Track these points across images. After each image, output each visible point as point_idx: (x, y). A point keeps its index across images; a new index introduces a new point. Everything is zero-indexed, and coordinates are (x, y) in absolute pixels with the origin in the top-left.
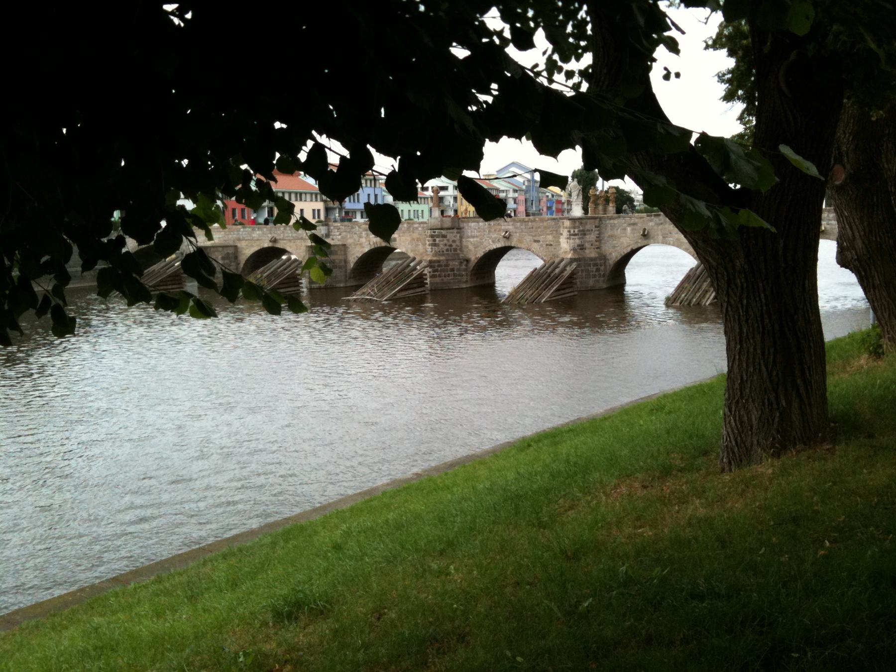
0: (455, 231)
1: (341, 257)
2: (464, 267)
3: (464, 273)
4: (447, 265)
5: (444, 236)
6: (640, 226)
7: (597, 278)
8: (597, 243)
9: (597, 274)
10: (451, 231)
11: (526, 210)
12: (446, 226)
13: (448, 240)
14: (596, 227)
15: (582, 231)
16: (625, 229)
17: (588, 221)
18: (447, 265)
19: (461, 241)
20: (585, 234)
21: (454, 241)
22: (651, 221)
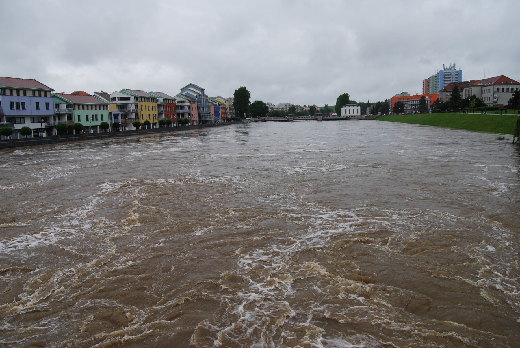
11: (198, 113)
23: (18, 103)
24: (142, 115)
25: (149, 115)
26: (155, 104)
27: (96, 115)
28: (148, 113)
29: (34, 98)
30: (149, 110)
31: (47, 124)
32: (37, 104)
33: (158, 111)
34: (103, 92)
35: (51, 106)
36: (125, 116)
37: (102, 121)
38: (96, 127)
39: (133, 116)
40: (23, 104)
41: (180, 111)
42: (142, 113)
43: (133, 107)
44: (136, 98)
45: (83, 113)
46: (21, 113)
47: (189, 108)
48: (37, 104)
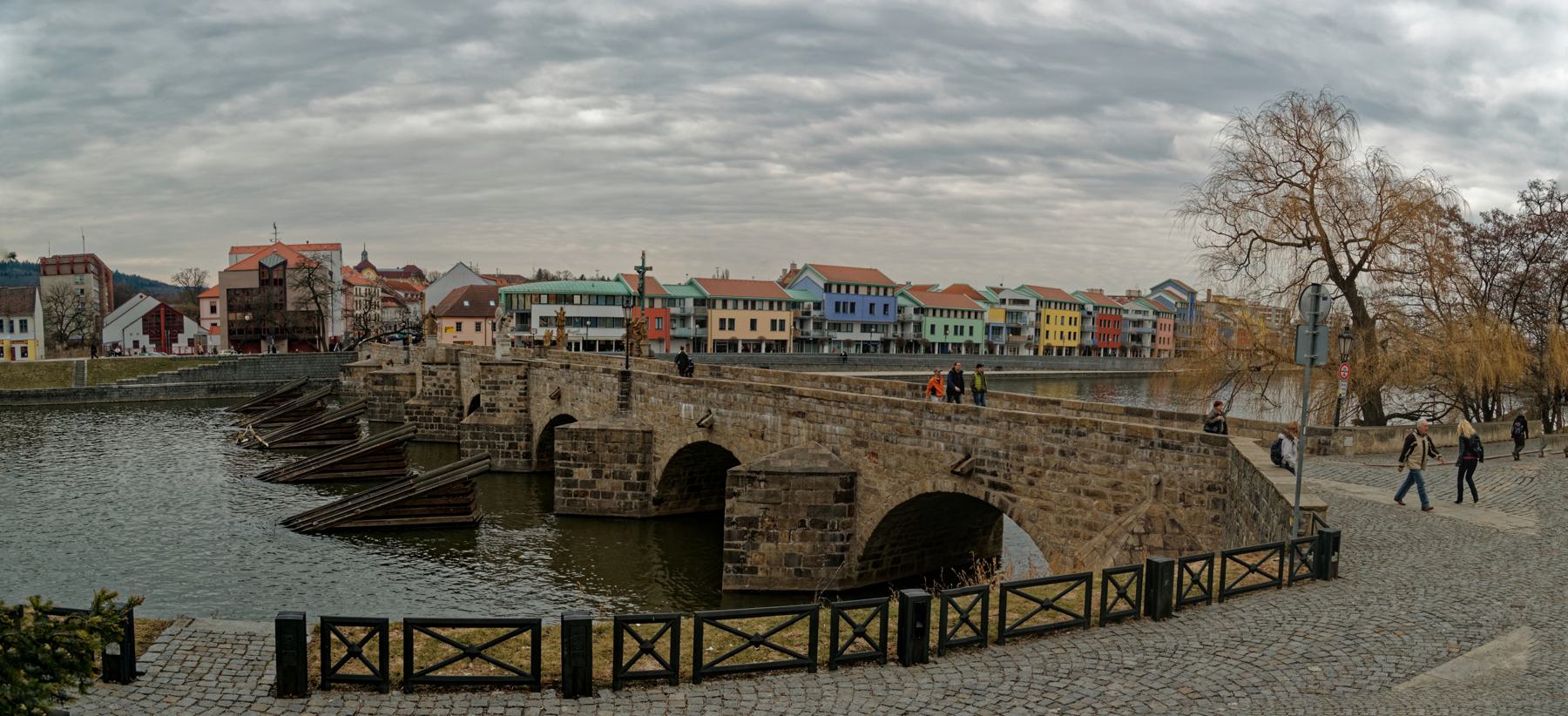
0: (449, 367)
1: (407, 389)
2: (454, 417)
3: (454, 425)
4: (430, 413)
5: (434, 374)
6: (555, 383)
7: (512, 459)
8: (522, 404)
9: (511, 451)
10: (444, 367)
11: (1174, 336)
12: (437, 360)
13: (438, 379)
14: (518, 377)
15: (492, 382)
16: (545, 385)
17: (504, 368)
18: (430, 413)
19: (458, 382)
20: (498, 388)
21: (447, 381)
22: (563, 375)
23: (844, 303)
24: (1047, 332)
25: (1062, 333)
26: (1077, 314)
27: (962, 327)
28: (1059, 328)
29: (869, 297)
30: (1062, 324)
31: (883, 335)
32: (872, 305)
33: (1082, 327)
34: (1004, 287)
35: (891, 309)
36: (1016, 331)
37: (971, 338)
38: (960, 344)
39: (1031, 332)
40: (853, 305)
41: (1132, 330)
42: (1047, 327)
43: (1032, 317)
44: (1040, 302)
45: (940, 322)
46: (848, 317)
47: (1155, 325)
48: (872, 305)
